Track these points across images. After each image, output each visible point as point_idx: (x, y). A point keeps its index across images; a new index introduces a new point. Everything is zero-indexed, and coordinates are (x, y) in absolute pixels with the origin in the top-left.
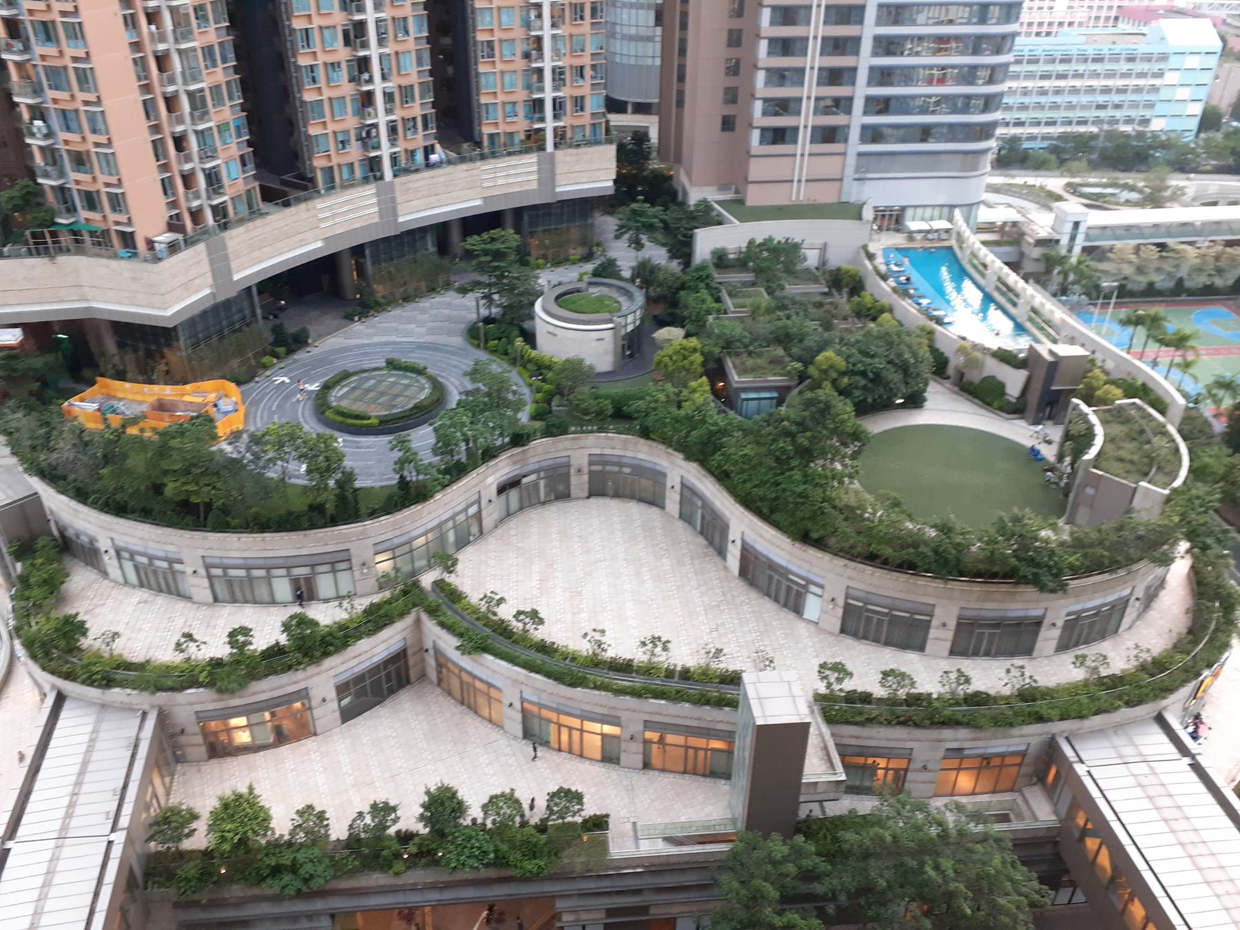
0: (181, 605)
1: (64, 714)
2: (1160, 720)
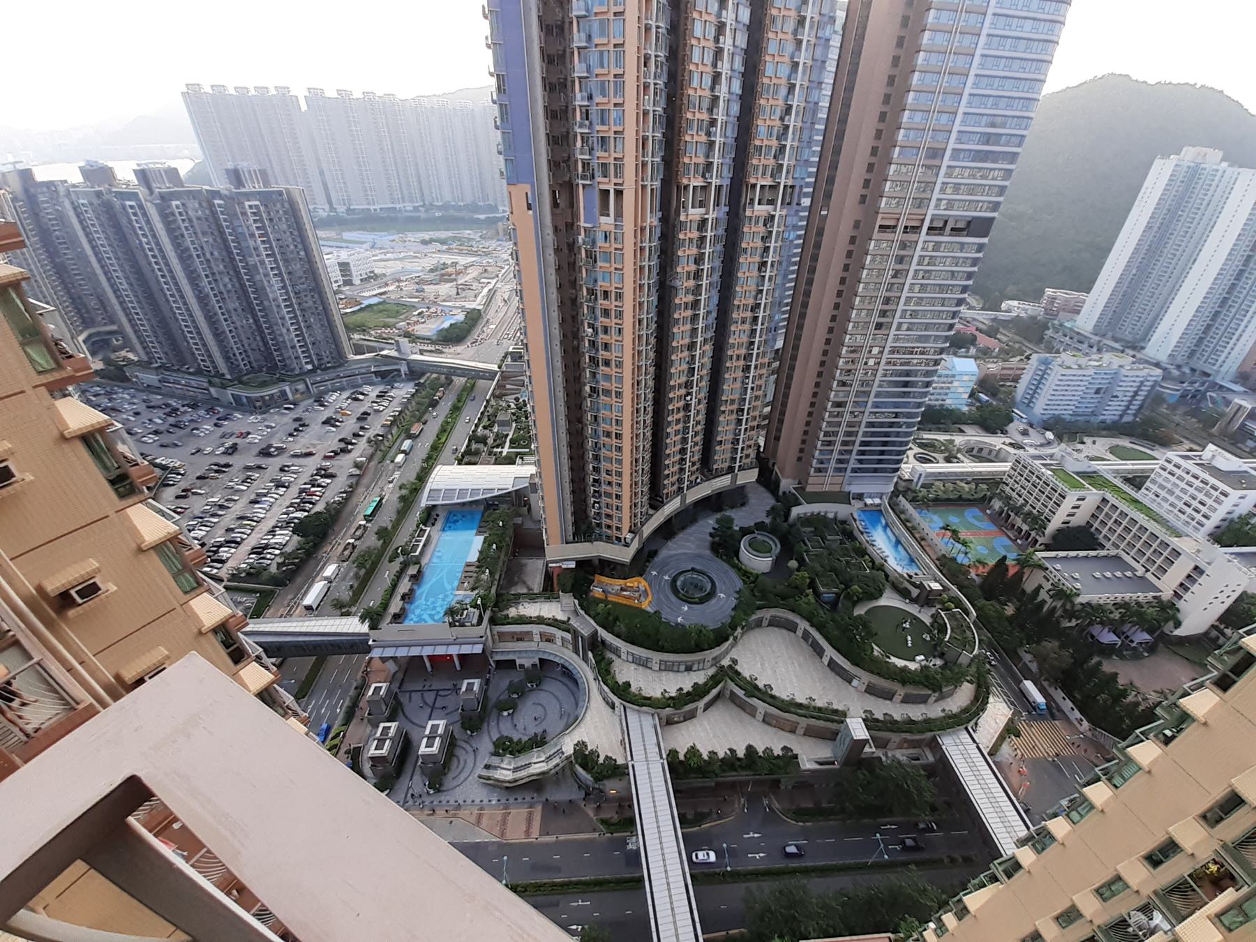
0: (648, 671)
2: (967, 729)
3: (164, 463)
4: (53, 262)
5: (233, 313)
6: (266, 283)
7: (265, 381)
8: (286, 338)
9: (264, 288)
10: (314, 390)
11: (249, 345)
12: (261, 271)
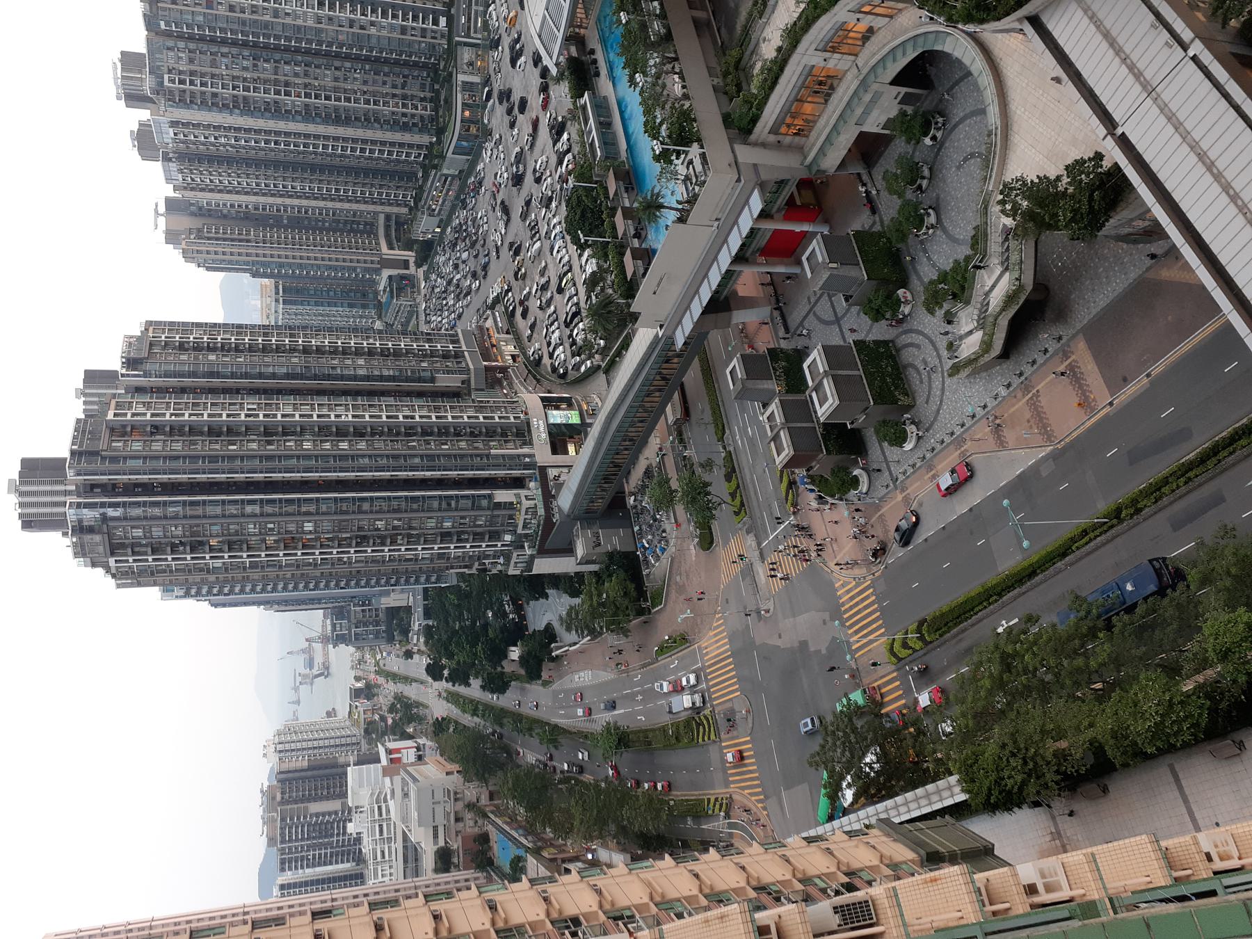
1: (1050, 27)
3: (495, 294)
4: (286, 227)
5: (342, 85)
6: (288, 20)
7: (446, 101)
8: (384, 33)
9: (299, 28)
10: (477, 38)
11: (394, 86)
12: (267, 18)
